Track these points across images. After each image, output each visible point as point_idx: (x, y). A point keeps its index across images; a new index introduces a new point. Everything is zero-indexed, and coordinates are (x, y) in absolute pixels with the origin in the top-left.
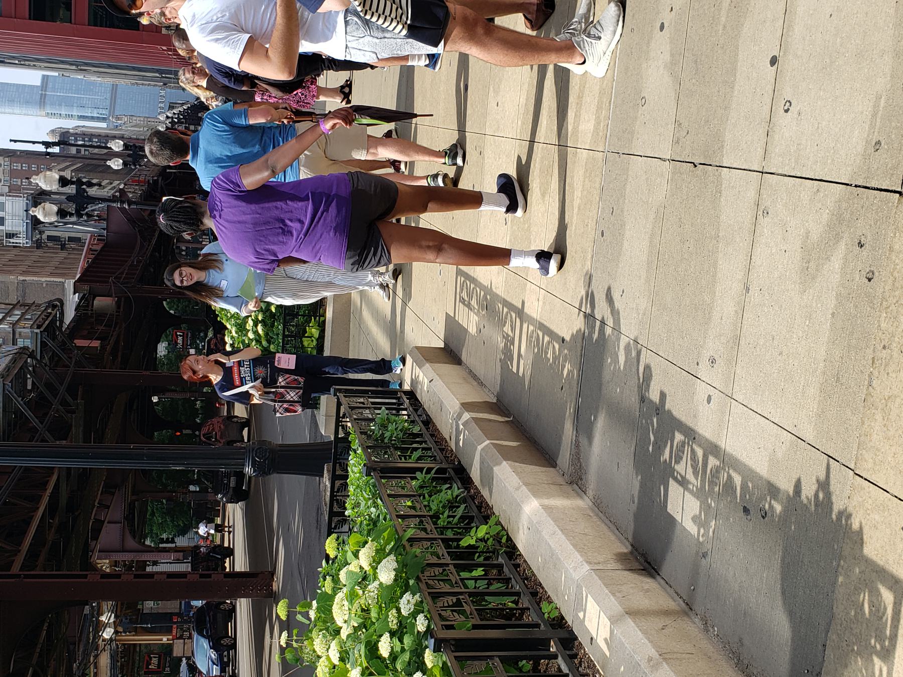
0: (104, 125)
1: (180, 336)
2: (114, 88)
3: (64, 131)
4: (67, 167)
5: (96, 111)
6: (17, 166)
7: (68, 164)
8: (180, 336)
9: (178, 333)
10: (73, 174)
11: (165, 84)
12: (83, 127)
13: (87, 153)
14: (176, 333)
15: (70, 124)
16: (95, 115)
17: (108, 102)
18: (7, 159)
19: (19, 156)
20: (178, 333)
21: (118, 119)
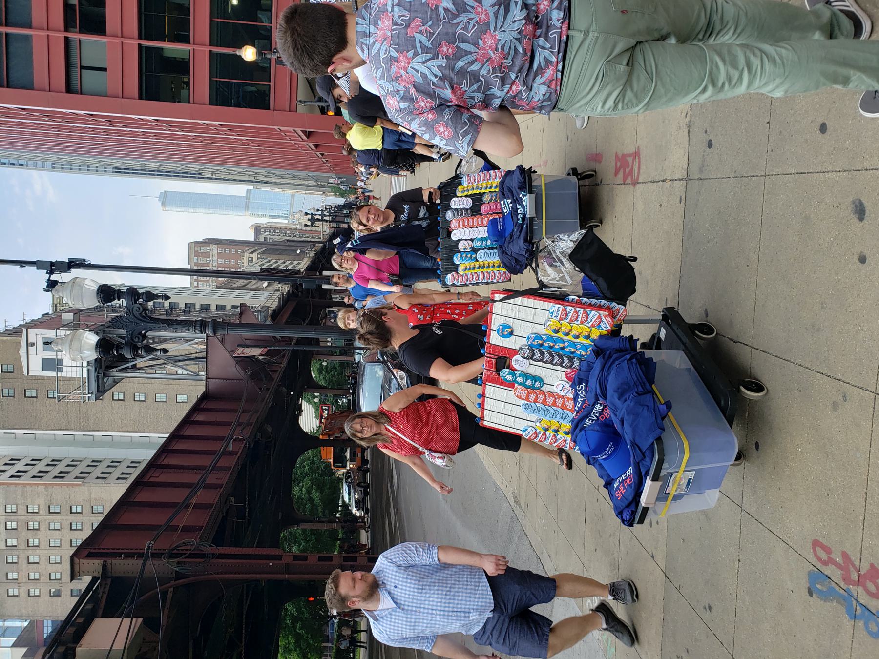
0: (286, 221)
1: (326, 409)
2: (293, 196)
3: (256, 225)
4: (255, 251)
5: (281, 212)
6: (221, 251)
7: (256, 248)
8: (326, 409)
9: (324, 407)
10: (259, 256)
11: (324, 193)
12: (272, 222)
13: (271, 240)
14: (322, 407)
15: (263, 221)
16: (281, 215)
17: (289, 207)
18: (215, 246)
19: (223, 244)
20: (324, 407)
21: (295, 217)
